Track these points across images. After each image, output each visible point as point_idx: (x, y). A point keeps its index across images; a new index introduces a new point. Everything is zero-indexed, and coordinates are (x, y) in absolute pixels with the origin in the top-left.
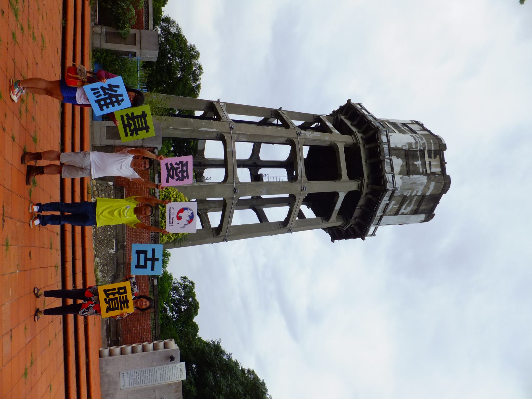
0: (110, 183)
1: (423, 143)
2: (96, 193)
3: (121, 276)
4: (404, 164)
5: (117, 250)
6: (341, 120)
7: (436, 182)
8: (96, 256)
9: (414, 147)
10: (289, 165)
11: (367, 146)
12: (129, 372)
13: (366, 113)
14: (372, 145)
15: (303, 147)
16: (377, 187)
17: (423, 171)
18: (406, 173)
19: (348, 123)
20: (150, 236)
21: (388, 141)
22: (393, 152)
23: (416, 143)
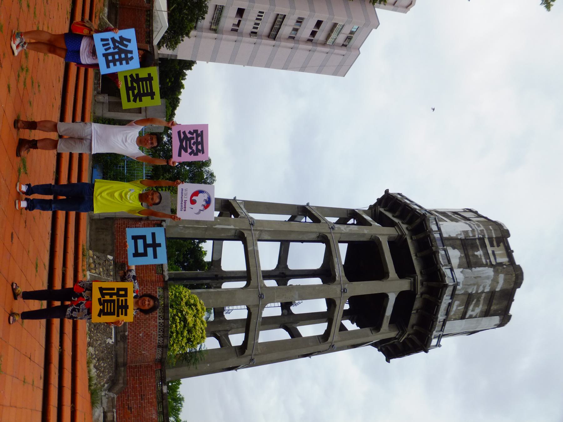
0: (109, 256)
1: (481, 230)
2: (93, 266)
3: (121, 381)
4: (463, 255)
5: (116, 341)
6: (381, 212)
7: (506, 275)
8: (89, 344)
9: (471, 235)
10: (326, 272)
11: (414, 238)
13: (408, 202)
14: (421, 236)
15: (339, 244)
16: (434, 284)
17: (486, 262)
18: (466, 265)
19: (390, 215)
20: (158, 324)
21: (439, 229)
22: (446, 242)
23: (473, 231)
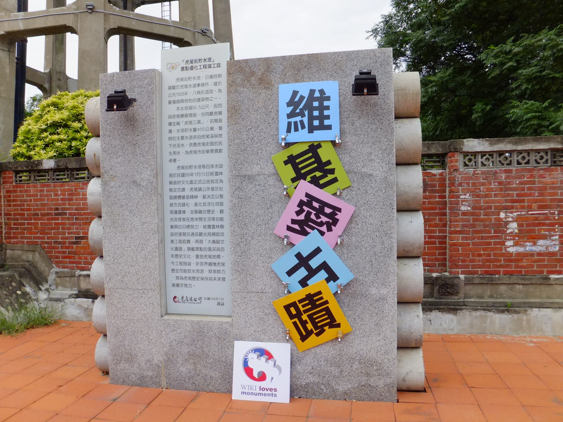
3: (30, 256)
12: (171, 278)
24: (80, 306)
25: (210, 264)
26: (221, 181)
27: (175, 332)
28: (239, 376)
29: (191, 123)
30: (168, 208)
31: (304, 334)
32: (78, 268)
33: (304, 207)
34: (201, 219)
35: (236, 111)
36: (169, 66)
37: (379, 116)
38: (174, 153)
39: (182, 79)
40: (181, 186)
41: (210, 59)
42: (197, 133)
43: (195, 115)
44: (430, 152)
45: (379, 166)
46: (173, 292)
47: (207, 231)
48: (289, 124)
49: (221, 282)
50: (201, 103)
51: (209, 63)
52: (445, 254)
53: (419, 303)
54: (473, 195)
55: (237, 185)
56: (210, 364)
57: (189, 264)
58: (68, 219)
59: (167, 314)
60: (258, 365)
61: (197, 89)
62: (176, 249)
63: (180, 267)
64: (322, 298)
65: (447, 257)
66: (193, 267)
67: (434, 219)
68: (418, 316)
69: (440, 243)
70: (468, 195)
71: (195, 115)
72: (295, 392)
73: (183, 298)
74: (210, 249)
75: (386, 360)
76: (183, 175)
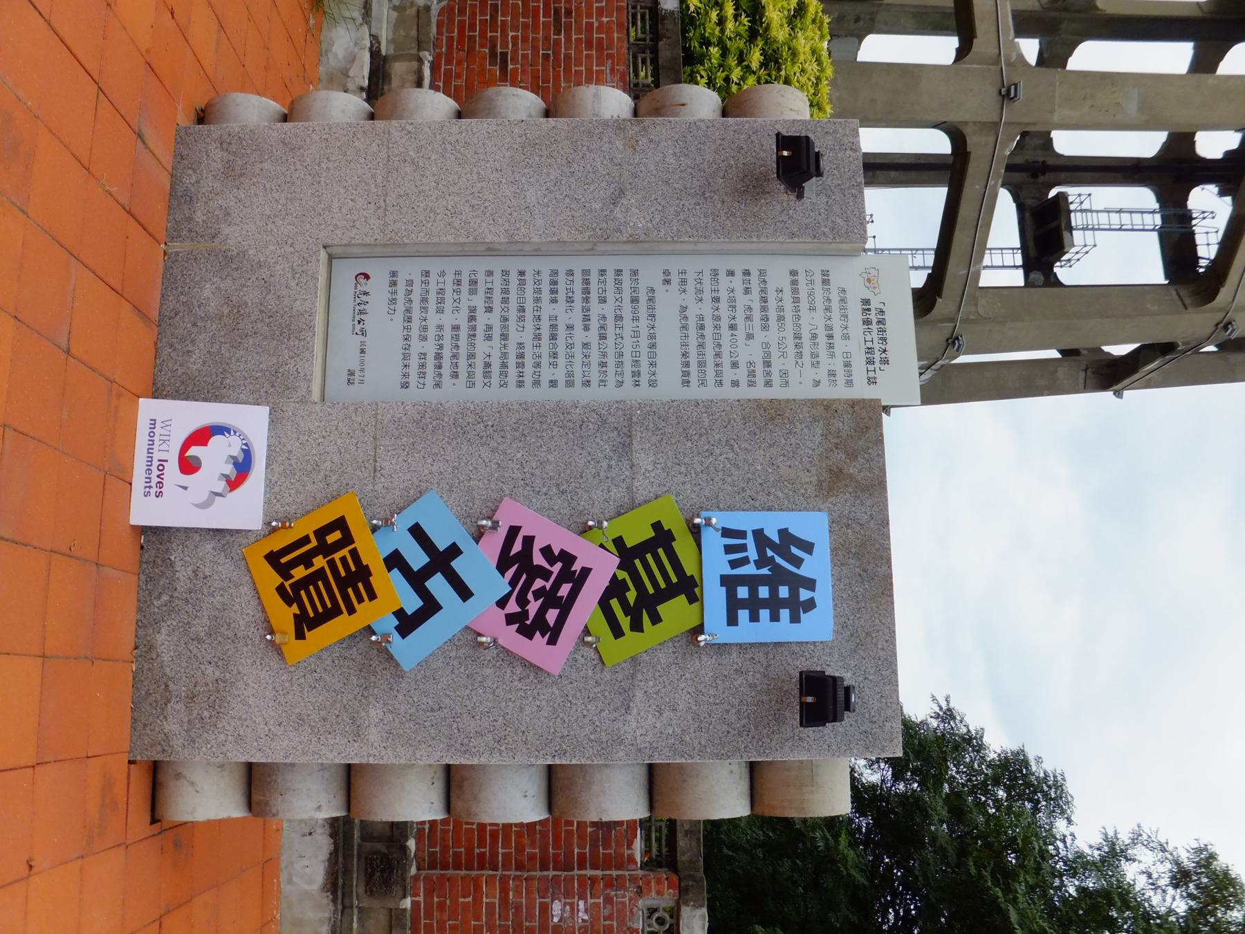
12: (409, 270)
24: (352, 59)
25: (438, 356)
26: (620, 384)
27: (290, 275)
28: (187, 415)
29: (748, 318)
30: (562, 264)
31: (283, 560)
32: (437, 58)
33: (559, 565)
34: (538, 337)
35: (772, 419)
36: (874, 272)
37: (756, 727)
38: (684, 282)
39: (843, 300)
40: (610, 295)
41: (885, 361)
42: (725, 332)
43: (765, 328)
44: (680, 835)
45: (648, 727)
46: (379, 272)
47: (512, 351)
48: (741, 534)
49: (399, 379)
50: (790, 342)
51: (877, 360)
52: (457, 866)
53: (349, 810)
54: (585, 927)
55: (611, 419)
56: (219, 351)
57: (440, 311)
58: (547, 38)
59: (331, 258)
60: (216, 457)
61: (822, 334)
62: (473, 282)
63: (433, 288)
64: (360, 600)
65: (450, 872)
66: (433, 319)
67: (533, 845)
68: (319, 808)
69: (482, 855)
70: (586, 917)
71: (765, 328)
72: (155, 538)
73: (366, 293)
74: (471, 356)
75: (222, 737)
76: (635, 300)
